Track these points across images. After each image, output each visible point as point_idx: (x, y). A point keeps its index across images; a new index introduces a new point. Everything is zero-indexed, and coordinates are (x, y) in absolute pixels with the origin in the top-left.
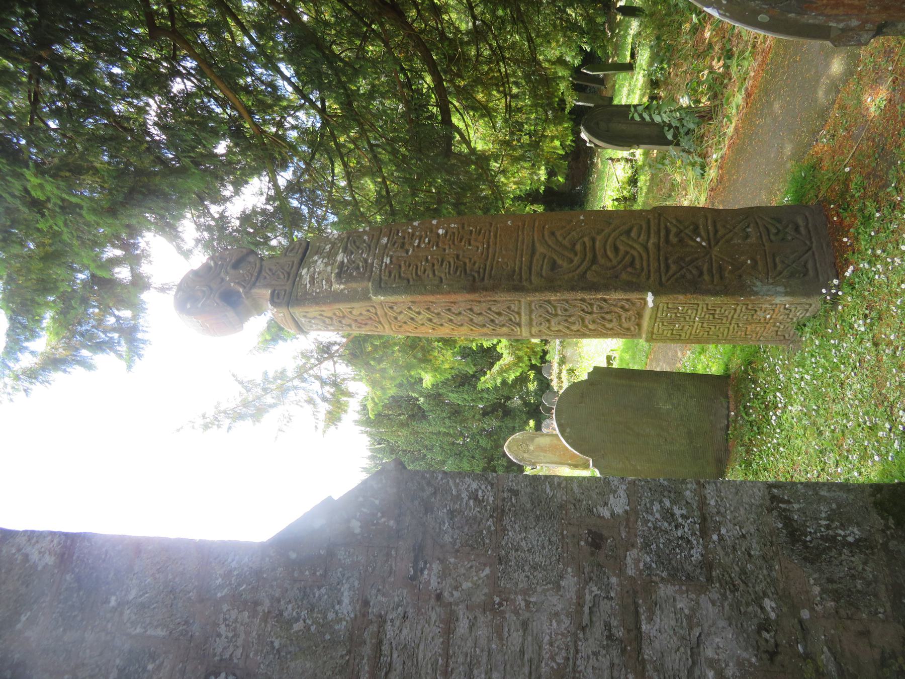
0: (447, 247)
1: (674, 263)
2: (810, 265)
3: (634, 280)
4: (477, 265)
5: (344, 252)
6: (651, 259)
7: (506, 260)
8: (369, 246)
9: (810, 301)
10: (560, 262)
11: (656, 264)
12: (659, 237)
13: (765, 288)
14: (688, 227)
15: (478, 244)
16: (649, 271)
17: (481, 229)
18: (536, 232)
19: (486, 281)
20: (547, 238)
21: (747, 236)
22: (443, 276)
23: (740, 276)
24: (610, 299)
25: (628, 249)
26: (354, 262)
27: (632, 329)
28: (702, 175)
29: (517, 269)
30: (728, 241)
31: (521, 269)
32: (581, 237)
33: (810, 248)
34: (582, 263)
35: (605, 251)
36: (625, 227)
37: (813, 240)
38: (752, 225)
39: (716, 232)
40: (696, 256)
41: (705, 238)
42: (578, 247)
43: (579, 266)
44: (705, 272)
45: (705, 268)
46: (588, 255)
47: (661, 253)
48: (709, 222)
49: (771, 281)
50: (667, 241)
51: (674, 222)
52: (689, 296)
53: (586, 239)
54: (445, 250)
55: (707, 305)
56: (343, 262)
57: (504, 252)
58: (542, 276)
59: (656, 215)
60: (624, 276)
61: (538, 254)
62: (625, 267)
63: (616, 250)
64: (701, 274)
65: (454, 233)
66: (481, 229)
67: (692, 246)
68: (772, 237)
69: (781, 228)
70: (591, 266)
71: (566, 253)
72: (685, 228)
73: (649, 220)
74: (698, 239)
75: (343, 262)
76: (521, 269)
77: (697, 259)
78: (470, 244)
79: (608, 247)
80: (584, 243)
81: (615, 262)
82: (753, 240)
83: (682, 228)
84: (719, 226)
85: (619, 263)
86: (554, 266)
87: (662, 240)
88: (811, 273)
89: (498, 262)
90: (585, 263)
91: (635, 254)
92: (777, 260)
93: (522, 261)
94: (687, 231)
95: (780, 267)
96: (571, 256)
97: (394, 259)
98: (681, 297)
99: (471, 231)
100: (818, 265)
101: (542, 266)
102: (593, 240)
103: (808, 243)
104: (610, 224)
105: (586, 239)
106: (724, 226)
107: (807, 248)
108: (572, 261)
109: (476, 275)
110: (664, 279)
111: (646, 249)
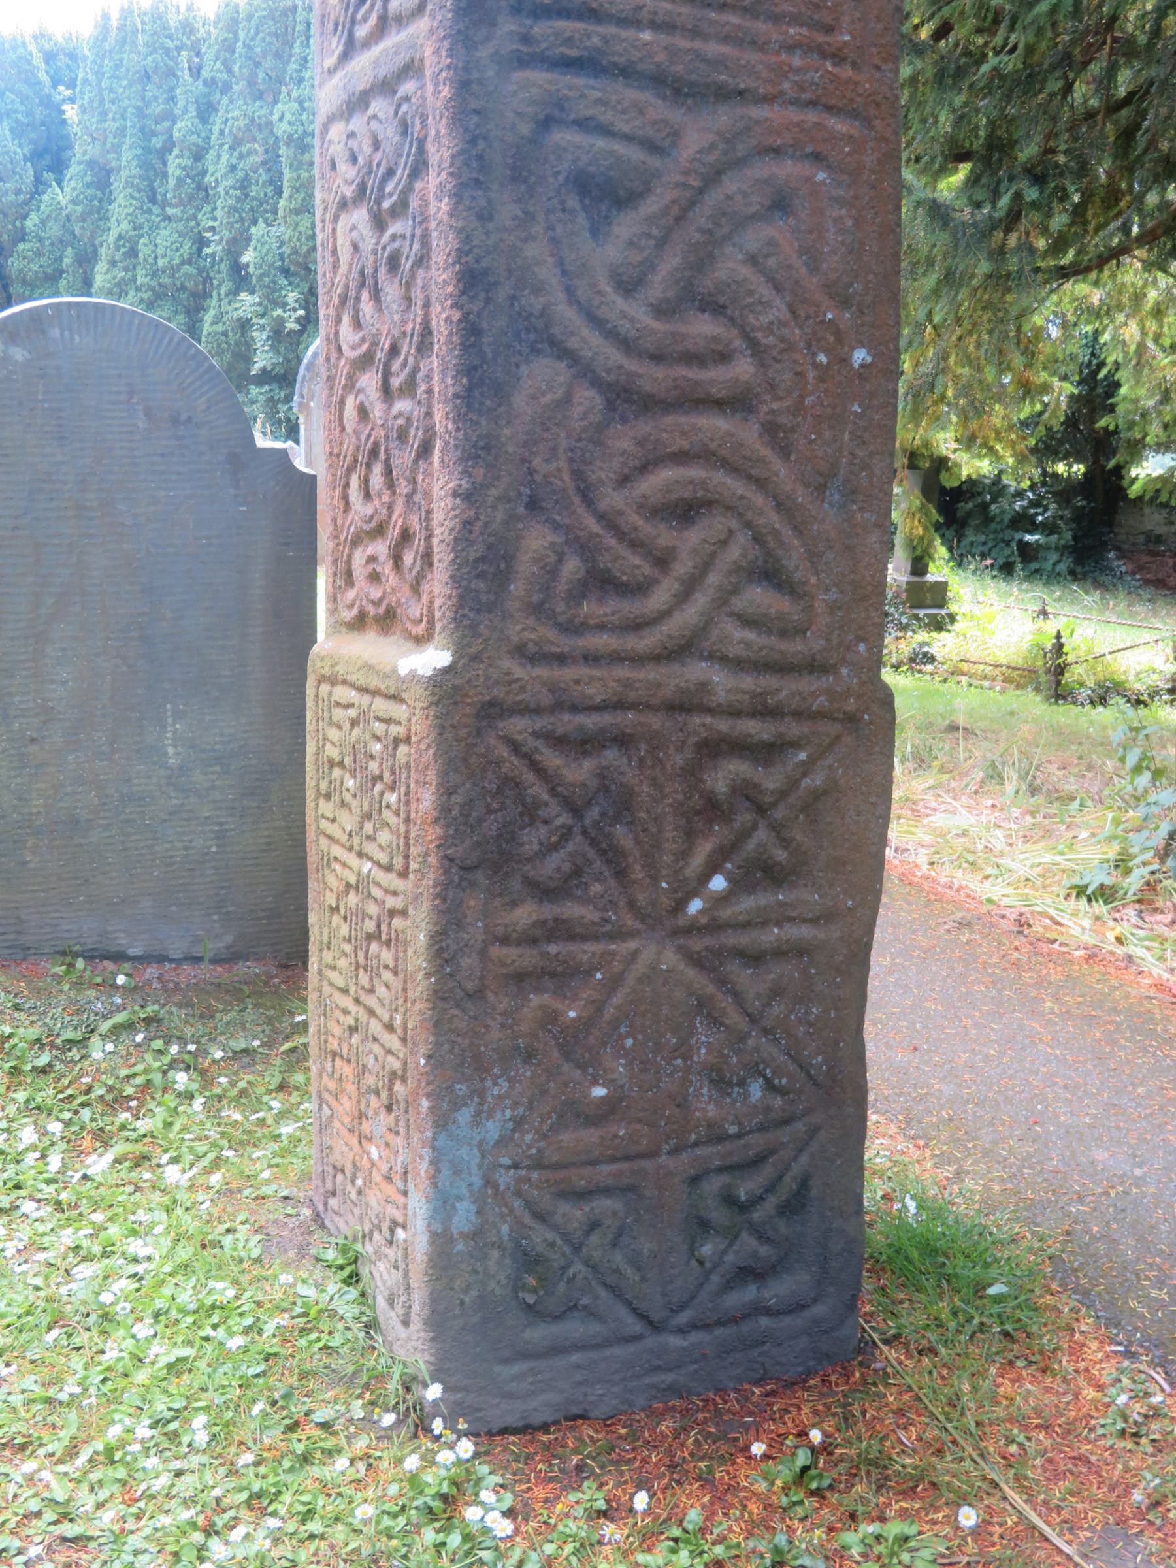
1: (602, 775)
2: (575, 1328)
3: (517, 588)
6: (623, 672)
9: (417, 1324)
10: (626, 226)
11: (595, 693)
13: (469, 1155)
14: (785, 843)
16: (561, 659)
18: (794, 115)
20: (762, 169)
21: (721, 1081)
23: (529, 1056)
24: (428, 474)
25: (683, 567)
27: (351, 594)
28: (1081, 891)
30: (703, 1005)
32: (753, 344)
33: (656, 1327)
35: (681, 457)
36: (794, 560)
37: (695, 1337)
38: (778, 1102)
39: (755, 958)
40: (638, 873)
41: (726, 913)
42: (703, 328)
43: (595, 321)
44: (549, 911)
45: (572, 910)
46: (660, 372)
47: (656, 721)
48: (805, 932)
49: (505, 1179)
50: (713, 749)
51: (817, 780)
52: (434, 833)
53: (743, 369)
55: (404, 913)
58: (546, 123)
59: (851, 704)
60: (537, 540)
61: (676, 116)
62: (586, 548)
63: (685, 511)
64: (546, 892)
67: (684, 855)
68: (714, 1185)
69: (757, 1215)
70: (596, 383)
71: (671, 262)
72: (777, 829)
74: (718, 883)
77: (621, 874)
79: (695, 472)
80: (724, 357)
81: (612, 499)
82: (707, 1105)
83: (779, 813)
84: (776, 971)
85: (608, 521)
86: (604, 194)
87: (723, 725)
88: (538, 1334)
90: (614, 356)
91: (659, 598)
92: (605, 1205)
94: (762, 834)
95: (573, 1215)
96: (658, 287)
98: (426, 800)
100: (575, 1358)
101: (606, 131)
103: (683, 1318)
104: (821, 489)
106: (776, 992)
107: (655, 1317)
108: (628, 286)
110: (518, 726)
111: (680, 650)
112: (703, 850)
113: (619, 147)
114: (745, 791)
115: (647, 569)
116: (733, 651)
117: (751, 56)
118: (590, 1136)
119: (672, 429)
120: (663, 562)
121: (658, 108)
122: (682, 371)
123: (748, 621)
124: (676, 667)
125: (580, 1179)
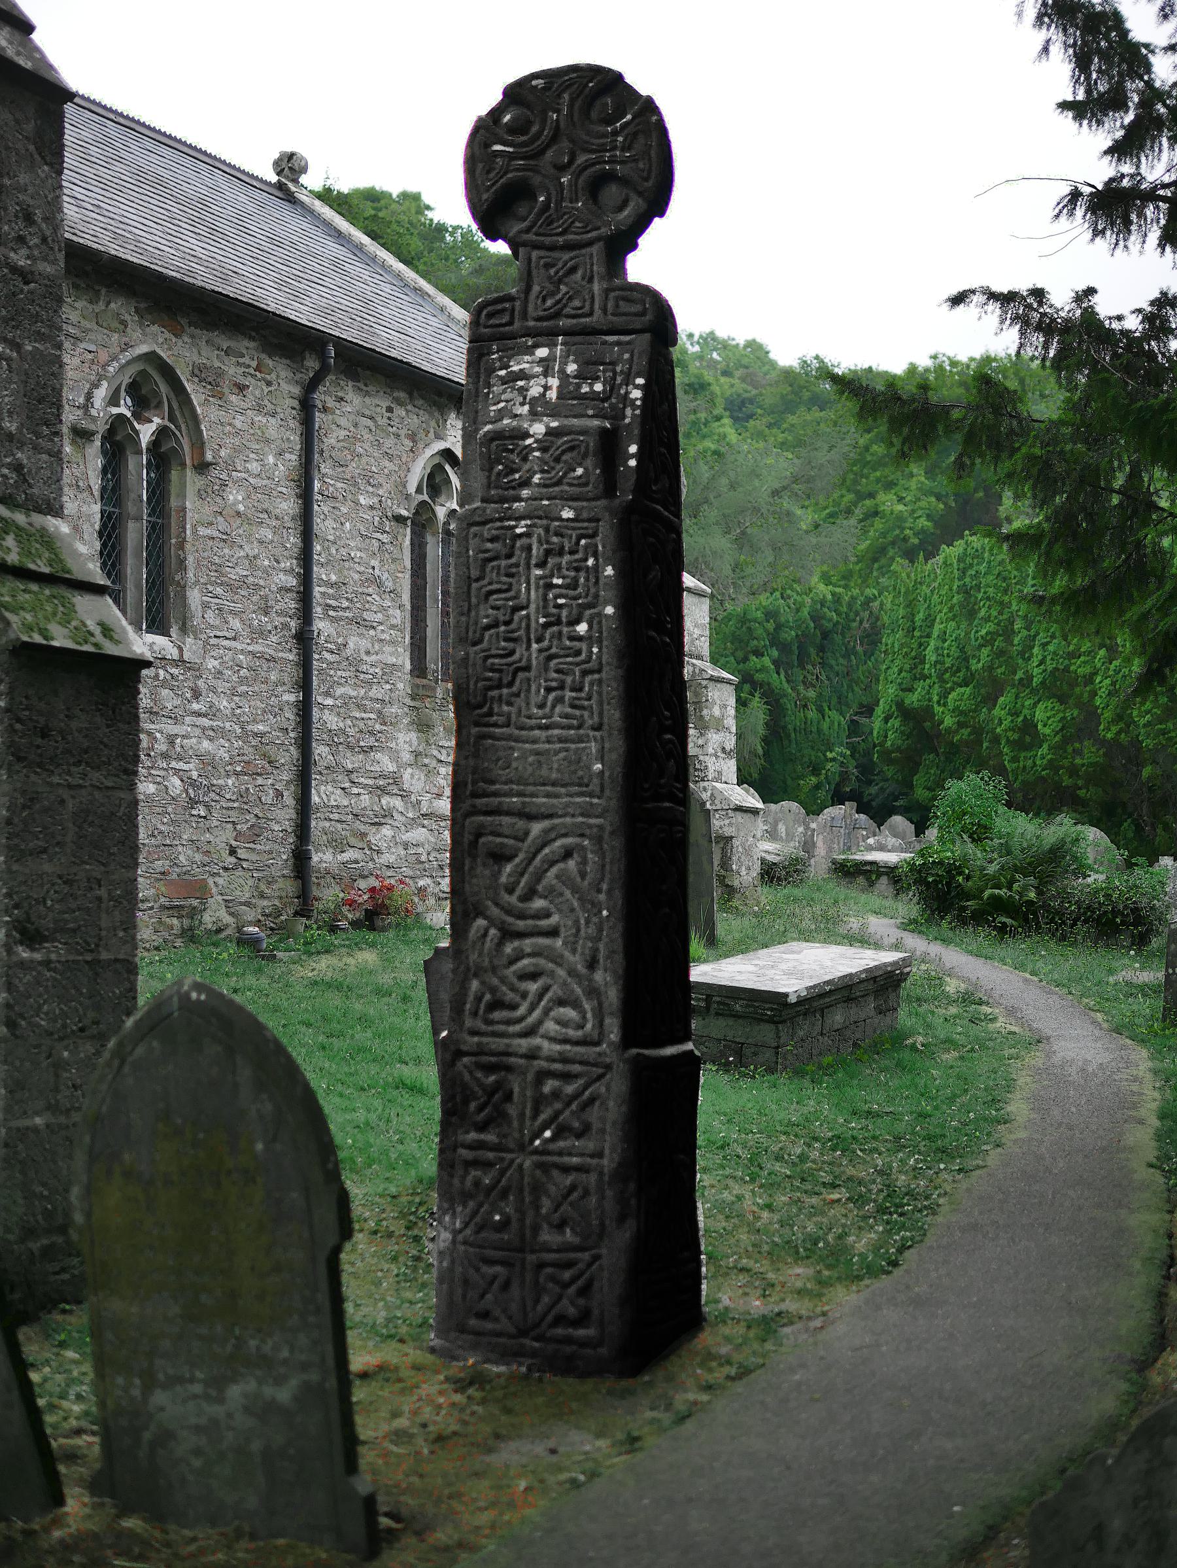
0: (546, 643)
2: (489, 1326)
4: (505, 708)
5: (550, 432)
6: (506, 1041)
7: (514, 765)
8: (559, 483)
10: (509, 868)
12: (554, 1061)
15: (547, 710)
17: (583, 708)
19: (475, 730)
22: (485, 645)
25: (530, 998)
26: (525, 459)
29: (494, 788)
31: (495, 794)
34: (502, 908)
39: (566, 1169)
40: (515, 1124)
41: (552, 1147)
42: (539, 904)
43: (497, 904)
50: (542, 1075)
53: (555, 919)
54: (539, 640)
56: (527, 435)
57: (531, 759)
59: (608, 1060)
62: (493, 990)
63: (533, 976)
65: (578, 653)
66: (583, 708)
73: (597, 1044)
74: (548, 1134)
75: (527, 435)
76: (495, 794)
78: (549, 690)
80: (548, 915)
82: (547, 1236)
89: (512, 749)
91: (522, 1010)
92: (498, 1269)
93: (510, 794)
96: (518, 892)
97: (524, 541)
99: (581, 690)
101: (499, 835)
102: (553, 933)
105: (555, 919)
108: (510, 891)
109: (485, 709)
111: (530, 1032)
112: (543, 1117)
113: (506, 840)
114: (556, 1094)
115: (518, 999)
116: (552, 1034)
117: (555, 801)
118: (496, 1236)
119: (528, 944)
120: (524, 996)
121: (521, 824)
122: (530, 922)
123: (559, 1022)
124: (529, 1040)
125: (490, 1253)
